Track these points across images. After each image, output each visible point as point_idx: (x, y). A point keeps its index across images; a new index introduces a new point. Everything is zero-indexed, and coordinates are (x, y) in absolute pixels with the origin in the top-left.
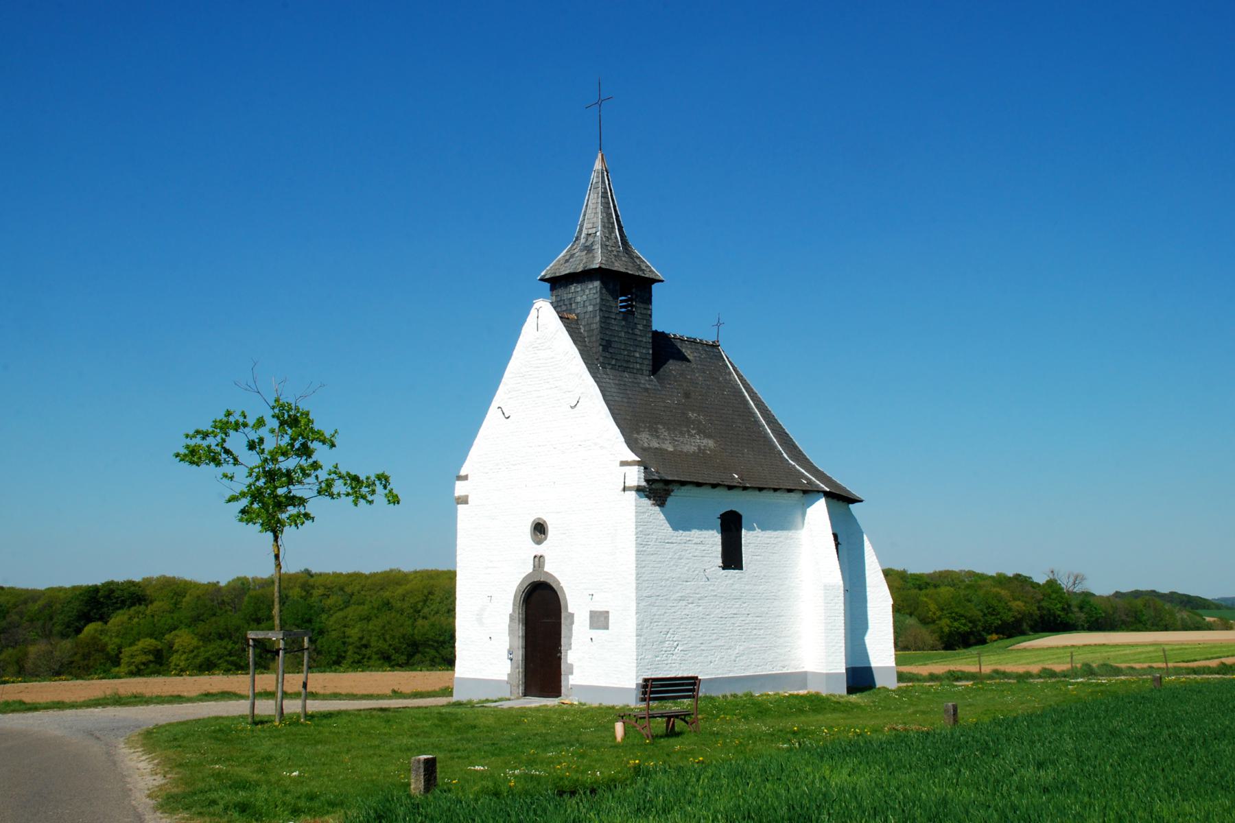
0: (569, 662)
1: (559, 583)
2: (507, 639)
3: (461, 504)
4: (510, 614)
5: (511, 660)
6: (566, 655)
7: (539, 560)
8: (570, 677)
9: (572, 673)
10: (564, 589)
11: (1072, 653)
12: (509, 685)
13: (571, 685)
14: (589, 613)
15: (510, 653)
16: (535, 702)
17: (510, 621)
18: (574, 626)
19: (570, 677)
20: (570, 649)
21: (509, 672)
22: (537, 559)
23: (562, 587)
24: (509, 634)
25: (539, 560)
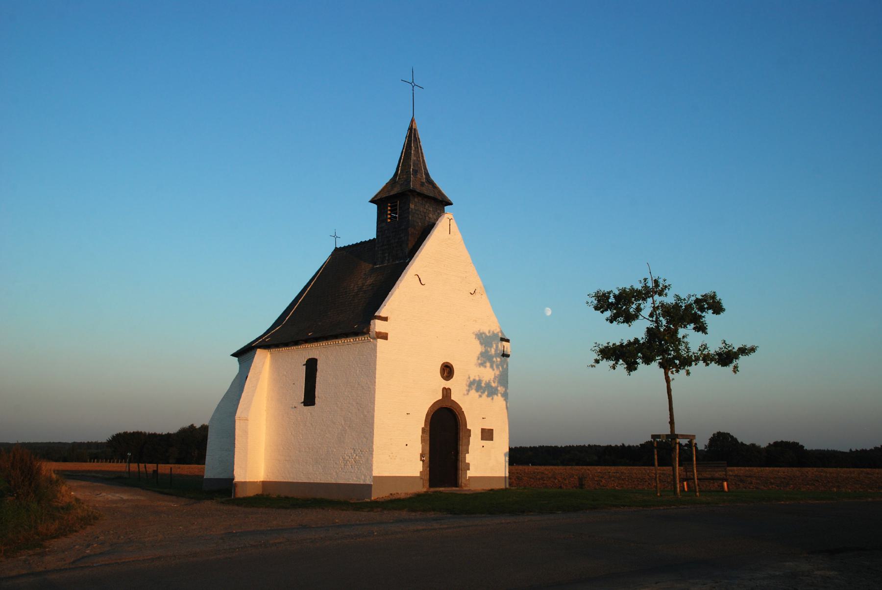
0: (467, 462)
1: (462, 409)
2: (421, 446)
3: (380, 338)
4: (422, 428)
5: (423, 461)
6: (465, 458)
7: (447, 392)
8: (468, 471)
9: (469, 469)
10: (465, 413)
11: (171, 468)
12: (422, 480)
13: (469, 477)
14: (480, 430)
15: (422, 455)
16: (432, 489)
17: (422, 433)
18: (471, 438)
19: (468, 471)
20: (468, 453)
21: (422, 470)
22: (445, 391)
23: (463, 412)
24: (422, 442)
25: (447, 392)
